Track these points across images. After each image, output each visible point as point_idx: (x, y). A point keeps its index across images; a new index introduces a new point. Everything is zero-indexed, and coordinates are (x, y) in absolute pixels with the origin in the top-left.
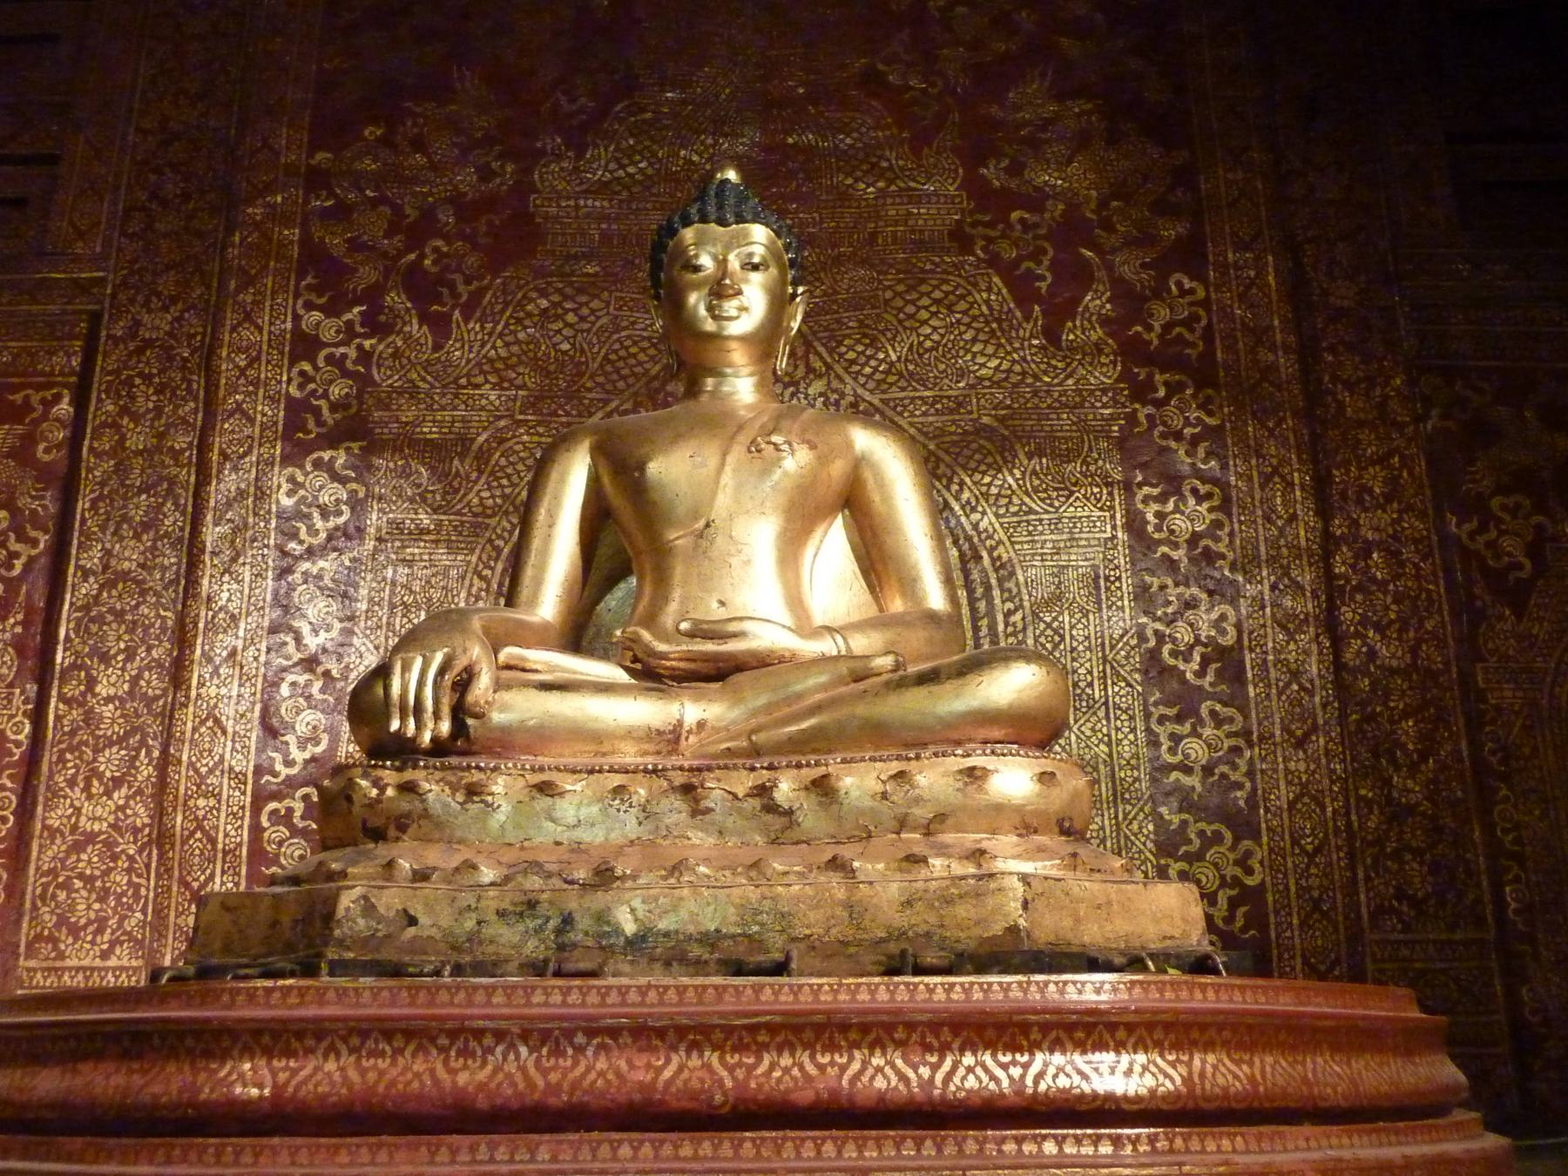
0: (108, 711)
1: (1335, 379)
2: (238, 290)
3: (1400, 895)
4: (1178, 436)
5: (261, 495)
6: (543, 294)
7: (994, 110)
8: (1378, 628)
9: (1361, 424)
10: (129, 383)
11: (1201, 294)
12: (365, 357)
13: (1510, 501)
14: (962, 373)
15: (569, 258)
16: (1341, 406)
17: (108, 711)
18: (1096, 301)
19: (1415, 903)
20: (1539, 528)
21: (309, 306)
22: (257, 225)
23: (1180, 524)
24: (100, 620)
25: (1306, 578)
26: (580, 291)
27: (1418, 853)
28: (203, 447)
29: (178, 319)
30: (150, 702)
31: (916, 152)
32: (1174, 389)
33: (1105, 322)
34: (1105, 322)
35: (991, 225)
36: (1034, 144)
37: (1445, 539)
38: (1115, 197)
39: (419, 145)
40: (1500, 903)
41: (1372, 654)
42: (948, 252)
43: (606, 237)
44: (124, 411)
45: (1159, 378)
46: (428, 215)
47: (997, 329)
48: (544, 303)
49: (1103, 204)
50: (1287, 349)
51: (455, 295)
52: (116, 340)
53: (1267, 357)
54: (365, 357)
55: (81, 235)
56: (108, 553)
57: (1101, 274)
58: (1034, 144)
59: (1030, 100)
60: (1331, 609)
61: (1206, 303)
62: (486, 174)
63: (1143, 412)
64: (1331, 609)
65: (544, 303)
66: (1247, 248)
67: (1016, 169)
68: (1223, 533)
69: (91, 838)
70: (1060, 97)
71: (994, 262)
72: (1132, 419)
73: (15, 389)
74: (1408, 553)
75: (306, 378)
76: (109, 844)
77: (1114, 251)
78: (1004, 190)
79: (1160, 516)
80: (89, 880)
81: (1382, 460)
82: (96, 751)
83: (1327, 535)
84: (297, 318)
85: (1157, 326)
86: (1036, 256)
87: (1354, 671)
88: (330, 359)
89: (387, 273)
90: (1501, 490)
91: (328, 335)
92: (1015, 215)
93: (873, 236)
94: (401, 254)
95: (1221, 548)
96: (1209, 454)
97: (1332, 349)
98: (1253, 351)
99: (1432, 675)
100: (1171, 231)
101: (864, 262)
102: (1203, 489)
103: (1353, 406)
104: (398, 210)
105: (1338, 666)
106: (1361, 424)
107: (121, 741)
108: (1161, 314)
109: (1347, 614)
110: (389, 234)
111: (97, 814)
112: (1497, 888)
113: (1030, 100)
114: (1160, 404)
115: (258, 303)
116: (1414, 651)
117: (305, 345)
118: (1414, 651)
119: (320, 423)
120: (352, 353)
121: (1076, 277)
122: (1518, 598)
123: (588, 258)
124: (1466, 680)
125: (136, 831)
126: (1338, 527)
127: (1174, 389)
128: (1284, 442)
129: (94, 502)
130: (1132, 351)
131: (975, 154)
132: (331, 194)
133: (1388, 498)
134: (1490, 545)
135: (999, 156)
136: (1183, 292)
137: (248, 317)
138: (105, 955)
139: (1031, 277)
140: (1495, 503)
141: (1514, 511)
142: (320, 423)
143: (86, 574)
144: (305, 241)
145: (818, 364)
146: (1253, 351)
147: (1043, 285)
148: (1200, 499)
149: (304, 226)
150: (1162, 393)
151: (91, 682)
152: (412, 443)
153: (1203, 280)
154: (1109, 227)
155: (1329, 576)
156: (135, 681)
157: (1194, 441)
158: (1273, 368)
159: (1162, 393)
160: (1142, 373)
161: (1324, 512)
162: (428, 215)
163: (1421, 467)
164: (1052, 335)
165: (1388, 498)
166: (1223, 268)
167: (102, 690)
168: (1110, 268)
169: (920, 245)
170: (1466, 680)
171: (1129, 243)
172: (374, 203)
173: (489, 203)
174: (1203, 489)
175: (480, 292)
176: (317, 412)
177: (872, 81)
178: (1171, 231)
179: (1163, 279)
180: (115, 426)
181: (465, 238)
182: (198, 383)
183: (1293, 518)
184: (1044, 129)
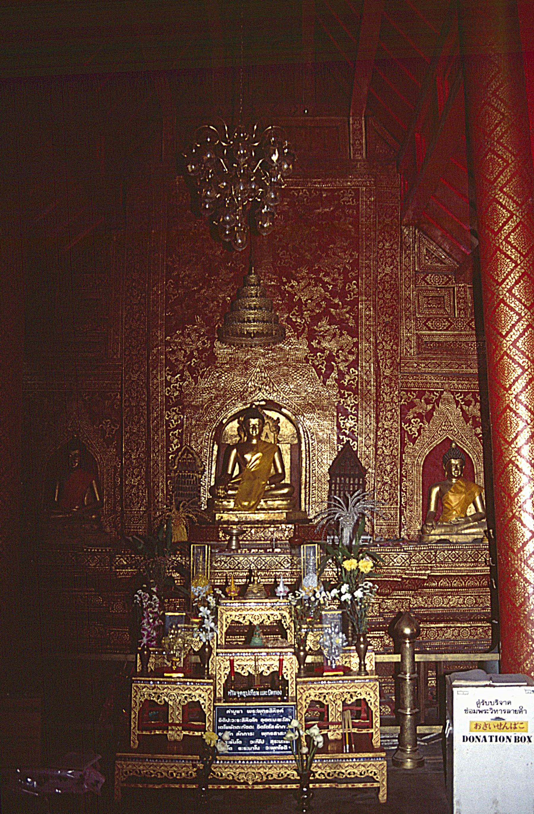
0: (134, 461)
1: (383, 392)
2: (153, 370)
3: (382, 499)
4: (349, 406)
5: (162, 417)
6: (217, 372)
7: (315, 327)
8: (386, 447)
9: (387, 402)
10: (130, 390)
11: (357, 373)
12: (180, 386)
13: (415, 420)
14: (306, 391)
15: (222, 364)
16: (384, 398)
17: (134, 461)
18: (334, 375)
19: (385, 500)
20: (421, 426)
21: (168, 374)
22: (155, 355)
23: (348, 425)
24: (130, 442)
25: (372, 436)
26: (225, 372)
27: (387, 491)
28: (148, 406)
29: (139, 376)
30: (142, 459)
31: (298, 339)
32: (349, 395)
33: (336, 380)
34: (336, 380)
35: (313, 356)
36: (324, 337)
37: (402, 428)
38: (340, 350)
39: (189, 335)
40: (401, 501)
41: (383, 452)
42: (303, 363)
43: (231, 358)
44: (130, 397)
45: (346, 393)
46: (192, 352)
47: (312, 381)
48: (217, 374)
49: (338, 351)
50: (374, 386)
51: (199, 373)
52: (127, 381)
53: (369, 387)
54: (180, 386)
55: (115, 354)
56: (130, 428)
57: (336, 368)
58: (324, 337)
59: (324, 325)
60: (376, 442)
61: (358, 375)
62: (204, 343)
63: (342, 400)
64: (376, 442)
65: (217, 374)
66: (368, 362)
67: (319, 343)
68: (356, 427)
69: (134, 486)
70: (330, 325)
71: (313, 365)
72: (340, 402)
73: (108, 392)
74: (393, 431)
75: (169, 391)
76: (138, 487)
77: (339, 363)
78: (316, 348)
79: (344, 423)
80: (135, 494)
81: (391, 411)
82: (133, 469)
83: (377, 427)
84: (166, 377)
85: (347, 381)
86: (322, 364)
87: (379, 455)
88: (173, 387)
89: (184, 366)
90: (414, 418)
91: (172, 382)
92: (318, 354)
93: (288, 359)
94: (187, 362)
95: (356, 430)
96: (355, 410)
97: (383, 385)
98: (366, 386)
99: (395, 456)
100: (351, 358)
101: (286, 365)
102: (353, 417)
103: (387, 398)
104: (185, 351)
105: (376, 454)
106: (387, 402)
107: (138, 467)
108: (348, 377)
109: (380, 443)
110: (184, 357)
111: (135, 481)
112: (401, 497)
113: (324, 325)
114: (346, 398)
115: (157, 373)
116: (392, 451)
117: (168, 384)
118: (392, 451)
119: (173, 401)
120: (178, 385)
121: (330, 369)
122: (414, 441)
123: (227, 363)
124: (401, 457)
125: (143, 485)
126: (380, 425)
127: (349, 395)
128: (371, 408)
129: (126, 418)
130: (341, 386)
131: (310, 339)
132: (171, 348)
133: (391, 419)
134: (410, 429)
135: (316, 339)
136: (353, 373)
137: (155, 377)
138: (140, 508)
139: (321, 369)
140: (412, 421)
141: (416, 423)
142: (173, 401)
143: (127, 433)
144: (166, 358)
145: (275, 389)
146: (366, 386)
147: (323, 371)
148: (352, 419)
149: (166, 356)
150: (346, 396)
151: (131, 455)
152: (192, 406)
153: (358, 370)
154: (339, 358)
155: (377, 435)
156: (139, 455)
157: (352, 407)
158: (370, 390)
159: (346, 396)
160: (342, 391)
161: (377, 423)
162: (192, 352)
163: (398, 413)
164: (324, 382)
165: (391, 419)
166: (362, 367)
167: (133, 457)
168: (337, 366)
169: (298, 361)
170: (401, 457)
171: (343, 361)
172: (180, 350)
173: (205, 350)
174: (353, 417)
175: (204, 372)
176: (172, 399)
177: (288, 320)
178: (351, 358)
179: (349, 370)
180: (129, 400)
181: (199, 358)
182: (145, 391)
183: (371, 424)
184: (325, 333)
